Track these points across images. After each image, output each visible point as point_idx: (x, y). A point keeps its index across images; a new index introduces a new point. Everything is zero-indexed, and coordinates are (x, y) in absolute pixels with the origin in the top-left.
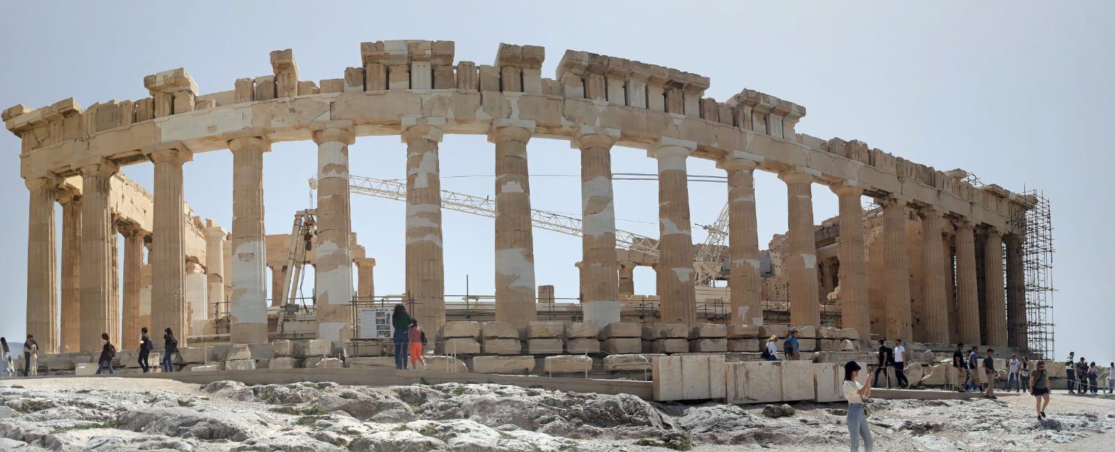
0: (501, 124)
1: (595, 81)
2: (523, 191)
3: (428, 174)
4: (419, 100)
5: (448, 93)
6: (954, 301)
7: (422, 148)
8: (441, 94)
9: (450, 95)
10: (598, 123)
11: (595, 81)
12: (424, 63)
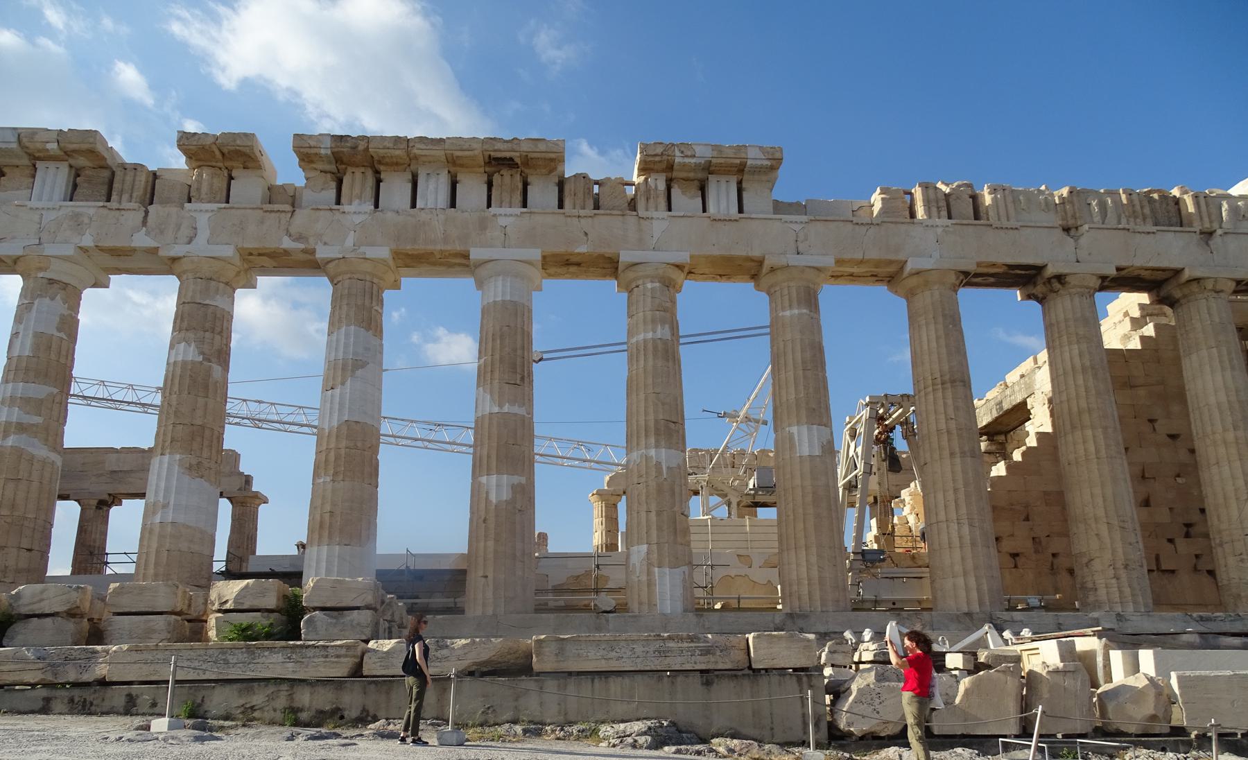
0: (172, 254)
1: (357, 181)
2: (200, 358)
3: (37, 335)
4: (36, 217)
5: (89, 208)
6: (397, 164)
7: (506, 520)
8: (78, 210)
9: (92, 211)
10: (350, 242)
11: (357, 181)
12: (58, 164)
